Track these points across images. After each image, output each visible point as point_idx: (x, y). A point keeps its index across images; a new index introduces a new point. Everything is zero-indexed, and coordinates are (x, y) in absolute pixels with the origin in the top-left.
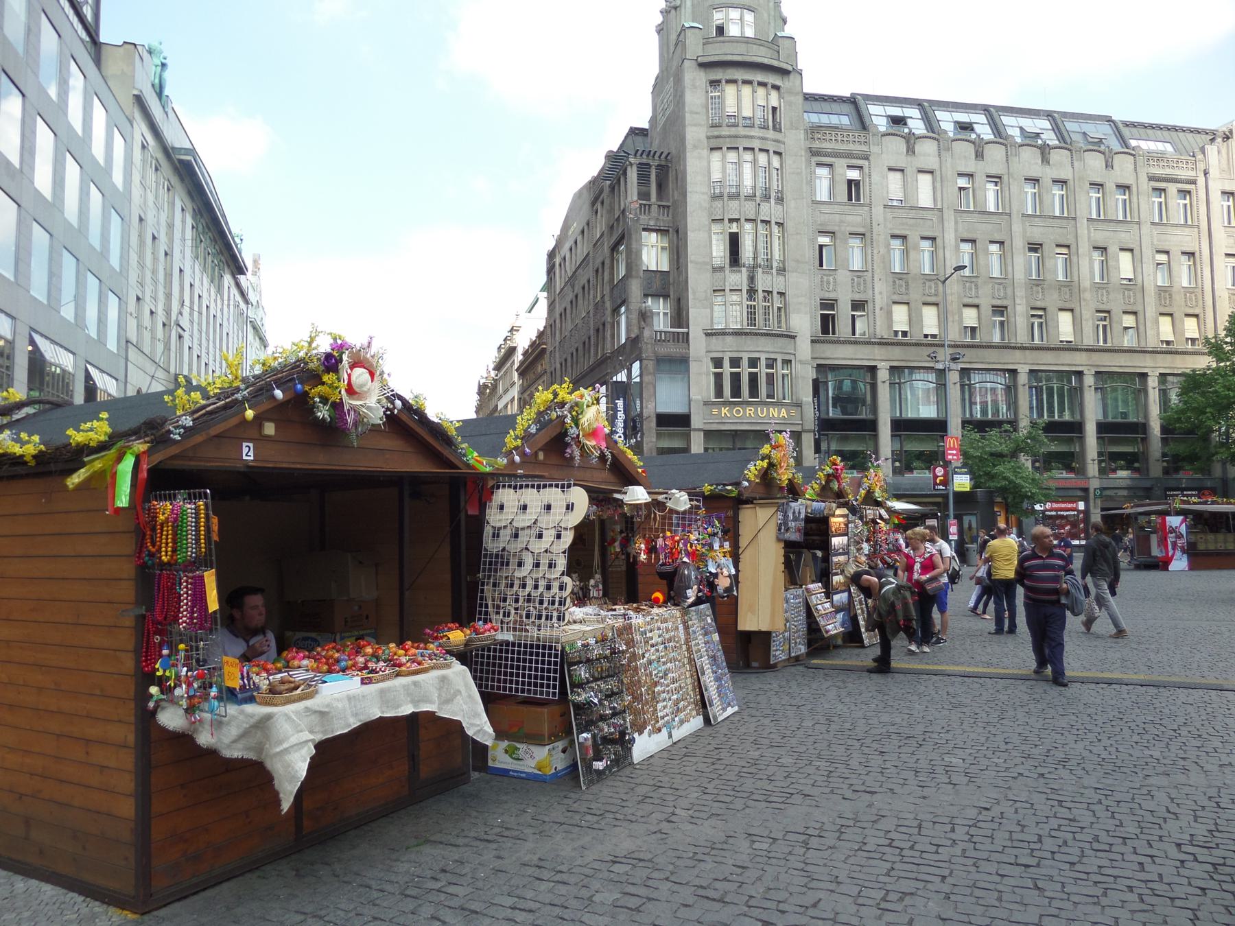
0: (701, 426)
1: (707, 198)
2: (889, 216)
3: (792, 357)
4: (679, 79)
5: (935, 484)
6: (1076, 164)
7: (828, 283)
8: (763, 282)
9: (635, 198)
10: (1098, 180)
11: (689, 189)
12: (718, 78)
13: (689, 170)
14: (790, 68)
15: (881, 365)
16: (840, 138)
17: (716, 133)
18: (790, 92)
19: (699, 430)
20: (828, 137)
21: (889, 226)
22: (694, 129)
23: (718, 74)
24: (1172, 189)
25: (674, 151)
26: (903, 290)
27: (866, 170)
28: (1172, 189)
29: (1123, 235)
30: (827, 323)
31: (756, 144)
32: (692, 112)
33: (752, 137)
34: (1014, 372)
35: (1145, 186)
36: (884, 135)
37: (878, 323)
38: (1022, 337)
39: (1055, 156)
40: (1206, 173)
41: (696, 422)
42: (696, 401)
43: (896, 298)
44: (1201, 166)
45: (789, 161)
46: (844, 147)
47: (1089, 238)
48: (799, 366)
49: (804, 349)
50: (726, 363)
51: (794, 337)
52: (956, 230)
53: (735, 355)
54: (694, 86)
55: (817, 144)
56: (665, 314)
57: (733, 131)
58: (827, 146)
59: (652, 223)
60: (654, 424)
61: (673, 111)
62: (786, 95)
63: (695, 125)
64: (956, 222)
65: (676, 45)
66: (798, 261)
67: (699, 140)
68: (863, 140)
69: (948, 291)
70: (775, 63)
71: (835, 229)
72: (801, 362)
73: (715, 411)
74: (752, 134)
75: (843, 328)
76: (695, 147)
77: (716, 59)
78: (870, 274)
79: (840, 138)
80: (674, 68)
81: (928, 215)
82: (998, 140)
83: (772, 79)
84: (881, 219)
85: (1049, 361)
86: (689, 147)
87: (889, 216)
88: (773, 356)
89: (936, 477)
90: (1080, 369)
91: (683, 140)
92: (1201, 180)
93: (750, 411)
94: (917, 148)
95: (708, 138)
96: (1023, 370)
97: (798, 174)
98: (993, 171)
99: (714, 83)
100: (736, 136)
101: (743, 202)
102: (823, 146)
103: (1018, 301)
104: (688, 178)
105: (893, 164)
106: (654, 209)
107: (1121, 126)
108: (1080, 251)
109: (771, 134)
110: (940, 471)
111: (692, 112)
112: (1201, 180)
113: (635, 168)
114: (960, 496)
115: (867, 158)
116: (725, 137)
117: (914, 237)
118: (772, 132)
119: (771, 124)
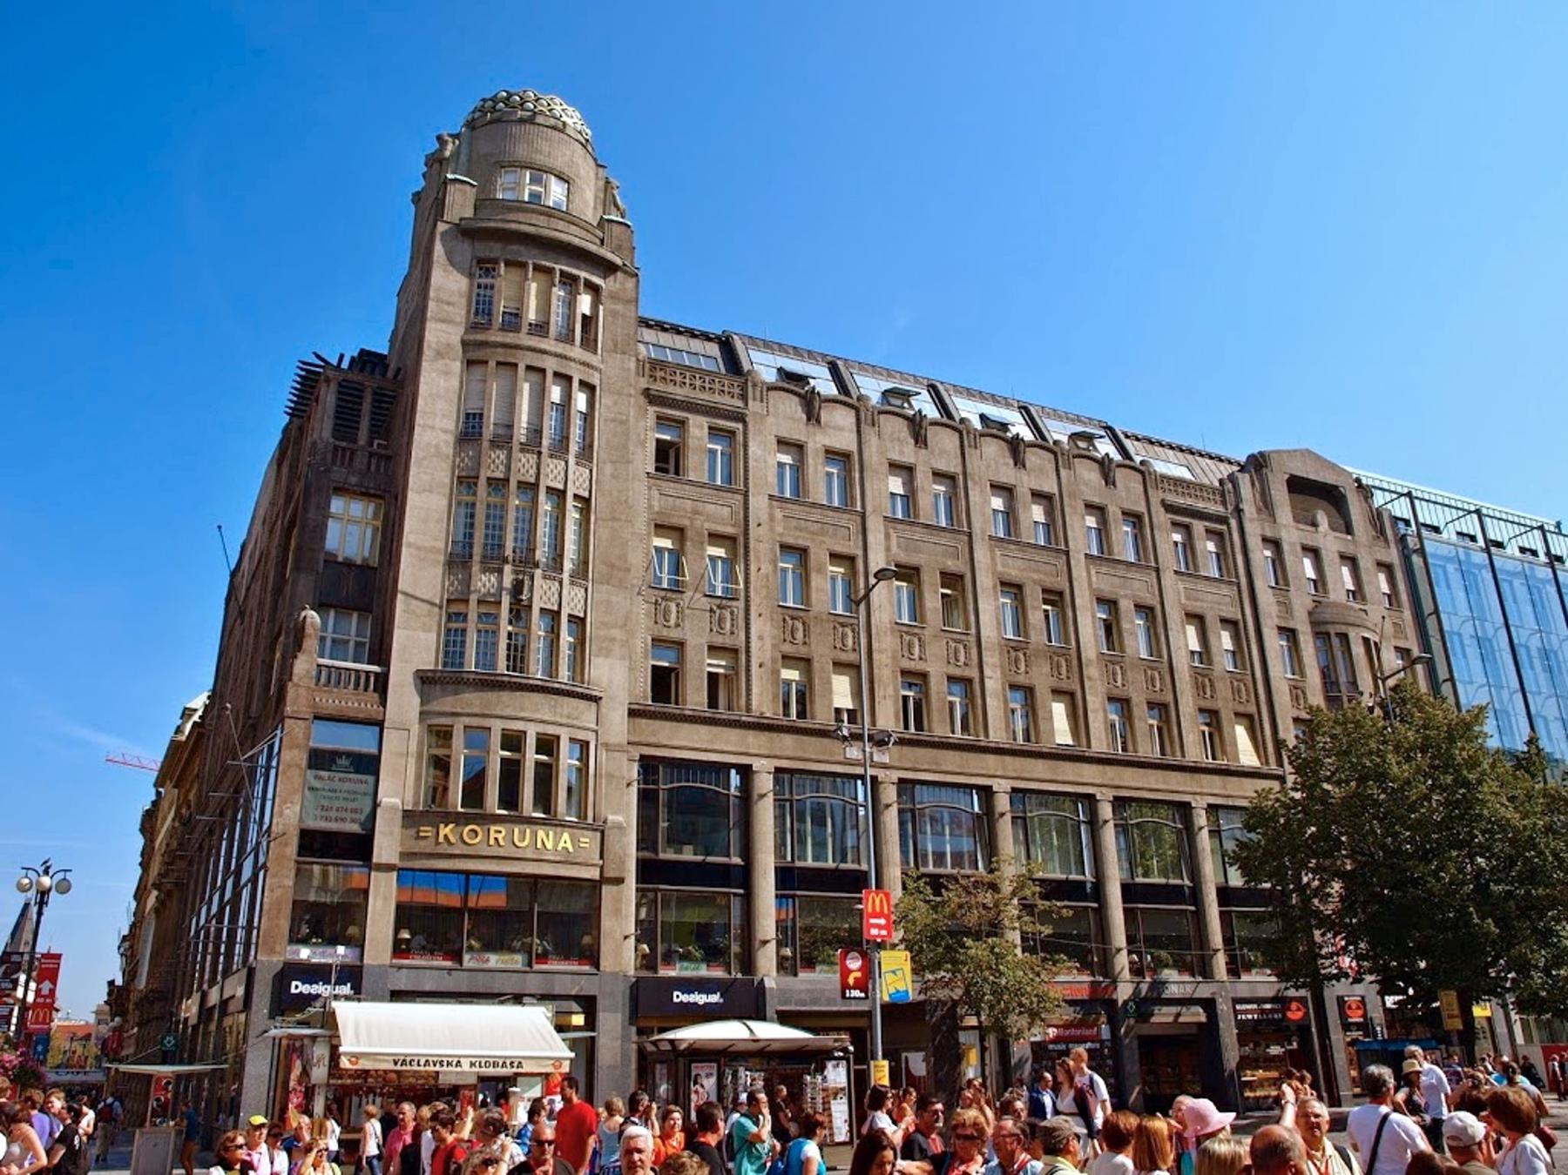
0: (395, 860)
1: (451, 439)
2: (779, 514)
3: (591, 737)
5: (845, 986)
6: (1063, 472)
7: (666, 613)
8: (542, 594)
9: (327, 434)
10: (1096, 500)
11: (419, 420)
15: (757, 764)
16: (698, 383)
19: (389, 868)
20: (678, 378)
21: (780, 529)
23: (495, 249)
24: (1198, 527)
26: (800, 635)
27: (740, 438)
28: (1198, 527)
29: (1137, 585)
30: (664, 683)
31: (550, 365)
32: (439, 300)
34: (987, 793)
35: (1162, 517)
36: (771, 388)
37: (755, 690)
38: (997, 735)
39: (1033, 458)
40: (1239, 512)
41: (386, 848)
42: (393, 808)
43: (788, 648)
44: (1230, 498)
45: (604, 401)
46: (706, 396)
47: (1090, 584)
48: (603, 754)
49: (617, 725)
50: (458, 740)
51: (596, 700)
52: (888, 549)
53: (475, 722)
55: (658, 387)
56: (358, 644)
58: (680, 393)
59: (353, 480)
60: (292, 849)
63: (443, 321)
64: (887, 536)
66: (612, 566)
68: (737, 391)
69: (875, 645)
71: (686, 522)
72: (606, 745)
73: (427, 831)
75: (695, 697)
76: (439, 355)
78: (741, 604)
79: (698, 383)
81: (844, 519)
82: (945, 420)
84: (764, 518)
85: (1039, 774)
86: (427, 352)
87: (779, 514)
88: (551, 730)
89: (846, 972)
90: (1091, 790)
92: (1233, 522)
93: (499, 832)
94: (824, 416)
95: (464, 343)
96: (1001, 786)
97: (622, 422)
98: (942, 466)
100: (517, 347)
101: (516, 454)
102: (670, 388)
103: (987, 672)
104: (420, 402)
105: (785, 434)
106: (360, 461)
107: (1122, 437)
108: (1078, 601)
109: (576, 352)
110: (854, 964)
111: (439, 300)
112: (1233, 522)
113: (333, 387)
114: (894, 1011)
115: (740, 418)
117: (819, 555)
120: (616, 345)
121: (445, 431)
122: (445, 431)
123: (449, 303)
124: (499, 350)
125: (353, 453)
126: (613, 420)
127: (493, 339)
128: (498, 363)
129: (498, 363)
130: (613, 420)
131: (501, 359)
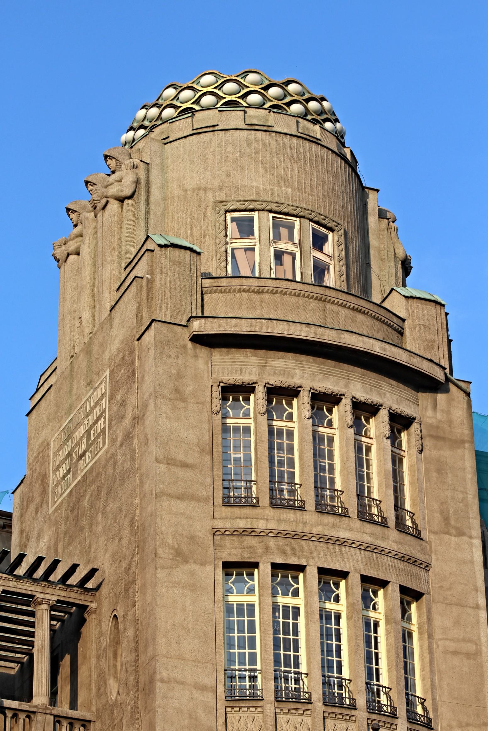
4: (127, 371)
12: (246, 378)
13: (163, 618)
14: (439, 375)
17: (241, 524)
18: (439, 436)
22: (179, 506)
25: (107, 569)
33: (343, 543)
54: (179, 395)
57: (288, 520)
61: (112, 459)
62: (428, 443)
63: (181, 497)
65: (122, 289)
67: (192, 538)
70: (401, 357)
74: (343, 534)
76: (180, 556)
77: (244, 328)
80: (114, 347)
83: (391, 396)
91: (140, 534)
97: (468, 655)
99: (236, 392)
100: (296, 536)
104: (161, 641)
109: (392, 540)
116: (267, 534)
118: (393, 534)
119: (391, 515)
120: (446, 519)
121: (203, 688)
122: (203, 688)
123: (185, 466)
124: (274, 543)
125: (30, 714)
126: (455, 653)
127: (262, 525)
128: (275, 566)
129: (275, 566)
130: (455, 653)
131: (279, 560)
